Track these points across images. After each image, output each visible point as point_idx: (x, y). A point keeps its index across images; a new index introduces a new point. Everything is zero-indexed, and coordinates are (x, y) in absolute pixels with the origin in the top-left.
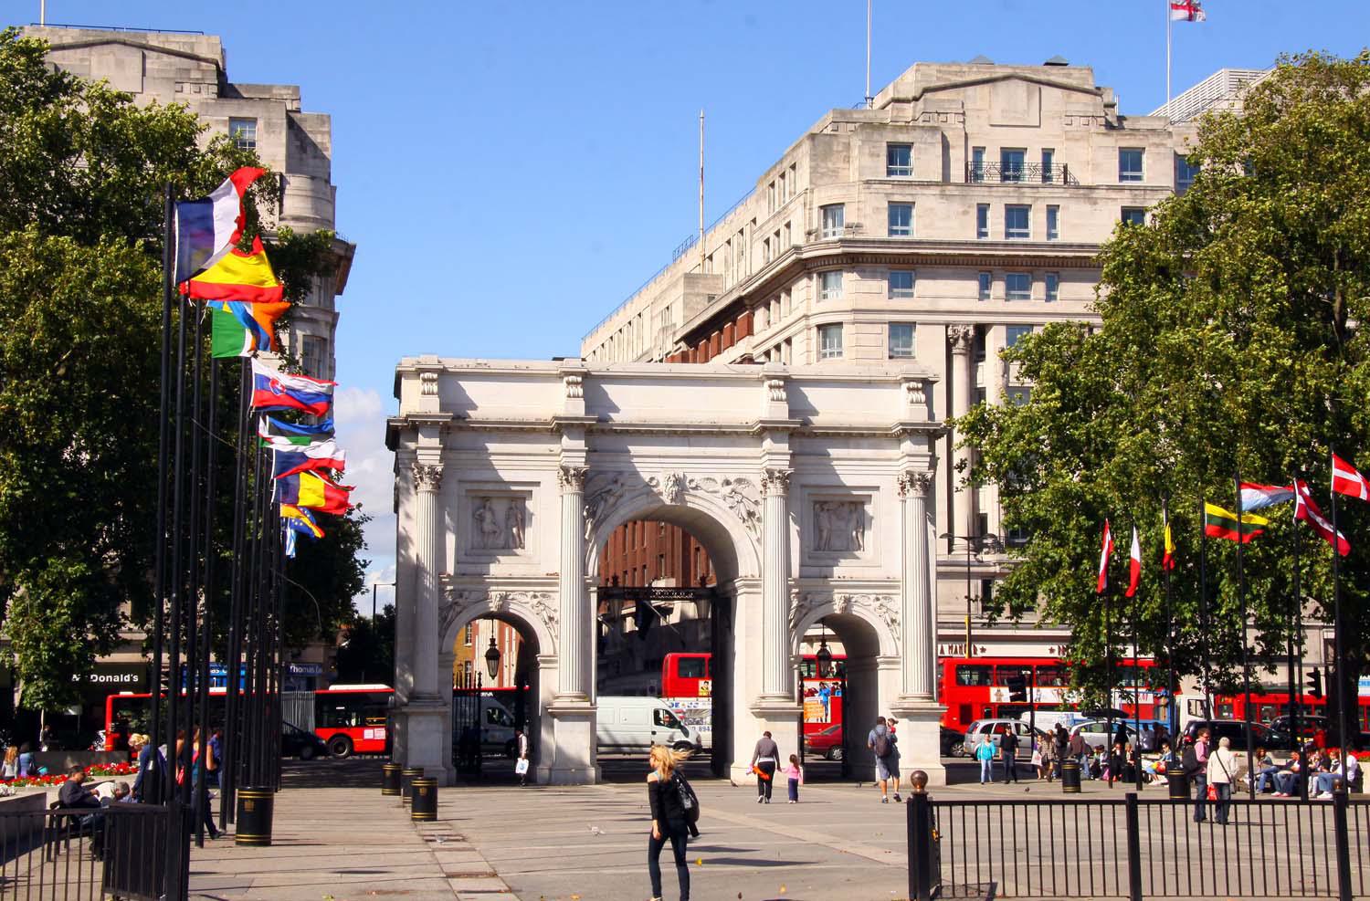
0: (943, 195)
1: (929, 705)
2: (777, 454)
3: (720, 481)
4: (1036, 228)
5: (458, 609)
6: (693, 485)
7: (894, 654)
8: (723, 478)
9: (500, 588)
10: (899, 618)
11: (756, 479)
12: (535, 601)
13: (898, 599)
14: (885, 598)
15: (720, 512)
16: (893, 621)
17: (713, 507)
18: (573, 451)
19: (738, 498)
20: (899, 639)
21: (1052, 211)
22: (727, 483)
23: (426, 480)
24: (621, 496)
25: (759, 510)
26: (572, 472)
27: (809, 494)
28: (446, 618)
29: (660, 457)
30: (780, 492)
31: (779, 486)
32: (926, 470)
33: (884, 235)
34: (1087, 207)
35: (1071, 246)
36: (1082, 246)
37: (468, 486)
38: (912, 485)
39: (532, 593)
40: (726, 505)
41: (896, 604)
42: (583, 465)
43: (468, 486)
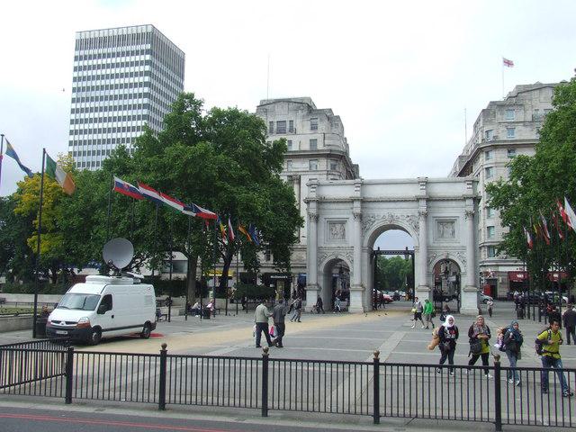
0: (524, 125)
33: (505, 139)
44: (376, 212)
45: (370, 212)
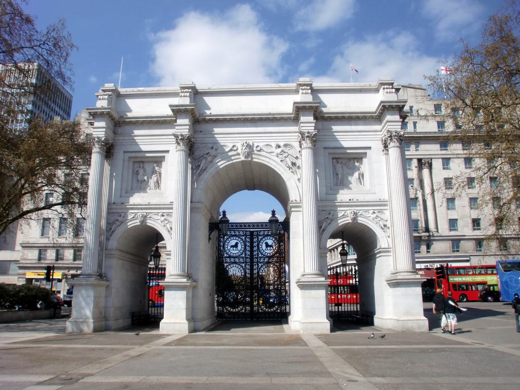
1: (413, 277)
2: (308, 123)
4: (410, 128)
5: (118, 223)
6: (259, 149)
7: (387, 247)
8: (276, 143)
9: (144, 211)
10: (388, 224)
11: (296, 145)
12: (163, 218)
13: (387, 213)
14: (379, 212)
15: (274, 164)
16: (385, 226)
17: (271, 161)
18: (183, 126)
19: (286, 155)
20: (389, 237)
21: (415, 123)
22: (279, 147)
23: (97, 146)
25: (298, 162)
26: (180, 137)
27: (329, 154)
28: (111, 229)
29: (238, 133)
30: (310, 145)
31: (308, 141)
32: (399, 130)
34: (425, 122)
35: (422, 132)
36: (426, 132)
37: (130, 155)
38: (391, 140)
39: (161, 213)
40: (278, 160)
41: (387, 215)
42: (187, 133)
43: (130, 155)
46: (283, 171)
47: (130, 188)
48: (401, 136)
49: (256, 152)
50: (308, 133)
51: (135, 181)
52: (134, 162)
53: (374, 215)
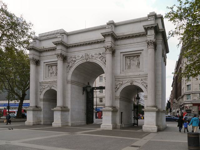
3: (98, 54)
15: (98, 62)
17: (97, 61)
22: (100, 54)
24: (75, 61)
32: (153, 39)
40: (100, 60)
44: (76, 54)
45: (73, 55)
46: (102, 64)
47: (47, 76)
48: (154, 42)
49: (91, 58)
50: (108, 47)
51: (49, 73)
52: (48, 66)
53: (142, 81)
